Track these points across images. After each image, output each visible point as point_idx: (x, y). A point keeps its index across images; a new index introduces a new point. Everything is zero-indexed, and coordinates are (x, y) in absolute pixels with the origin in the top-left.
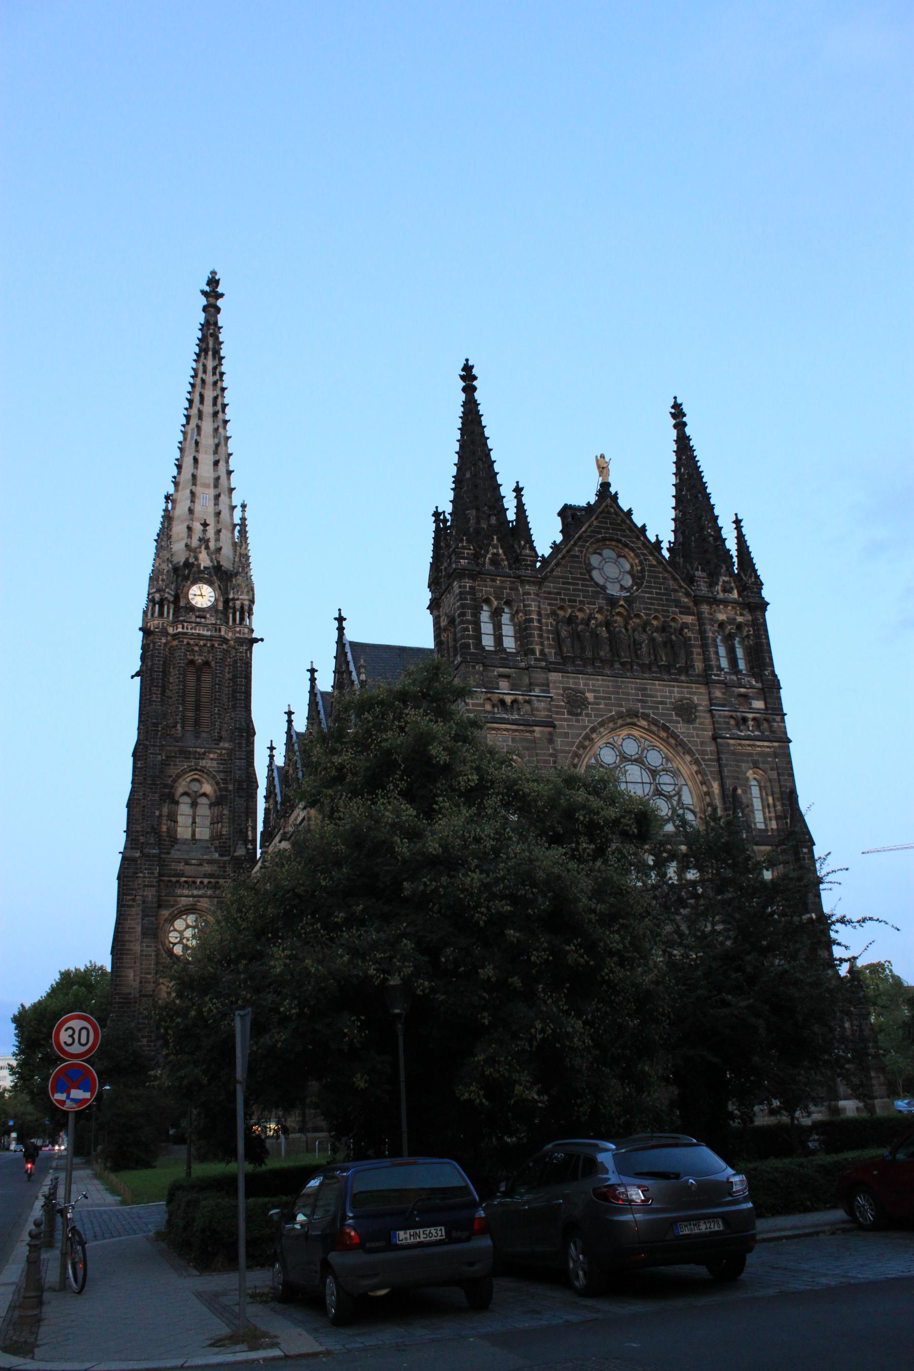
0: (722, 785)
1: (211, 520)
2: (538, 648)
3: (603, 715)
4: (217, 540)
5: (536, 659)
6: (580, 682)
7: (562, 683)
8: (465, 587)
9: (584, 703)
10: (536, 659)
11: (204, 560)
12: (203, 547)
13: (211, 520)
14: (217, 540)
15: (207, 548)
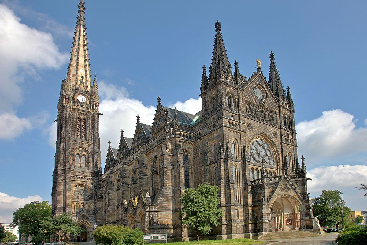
0: (282, 155)
1: (84, 77)
2: (242, 110)
3: (256, 132)
4: (86, 84)
5: (242, 113)
6: (252, 122)
7: (247, 121)
8: (223, 87)
9: (252, 128)
10: (242, 113)
11: (82, 89)
12: (82, 84)
13: (84, 77)
14: (86, 84)
15: (83, 85)
